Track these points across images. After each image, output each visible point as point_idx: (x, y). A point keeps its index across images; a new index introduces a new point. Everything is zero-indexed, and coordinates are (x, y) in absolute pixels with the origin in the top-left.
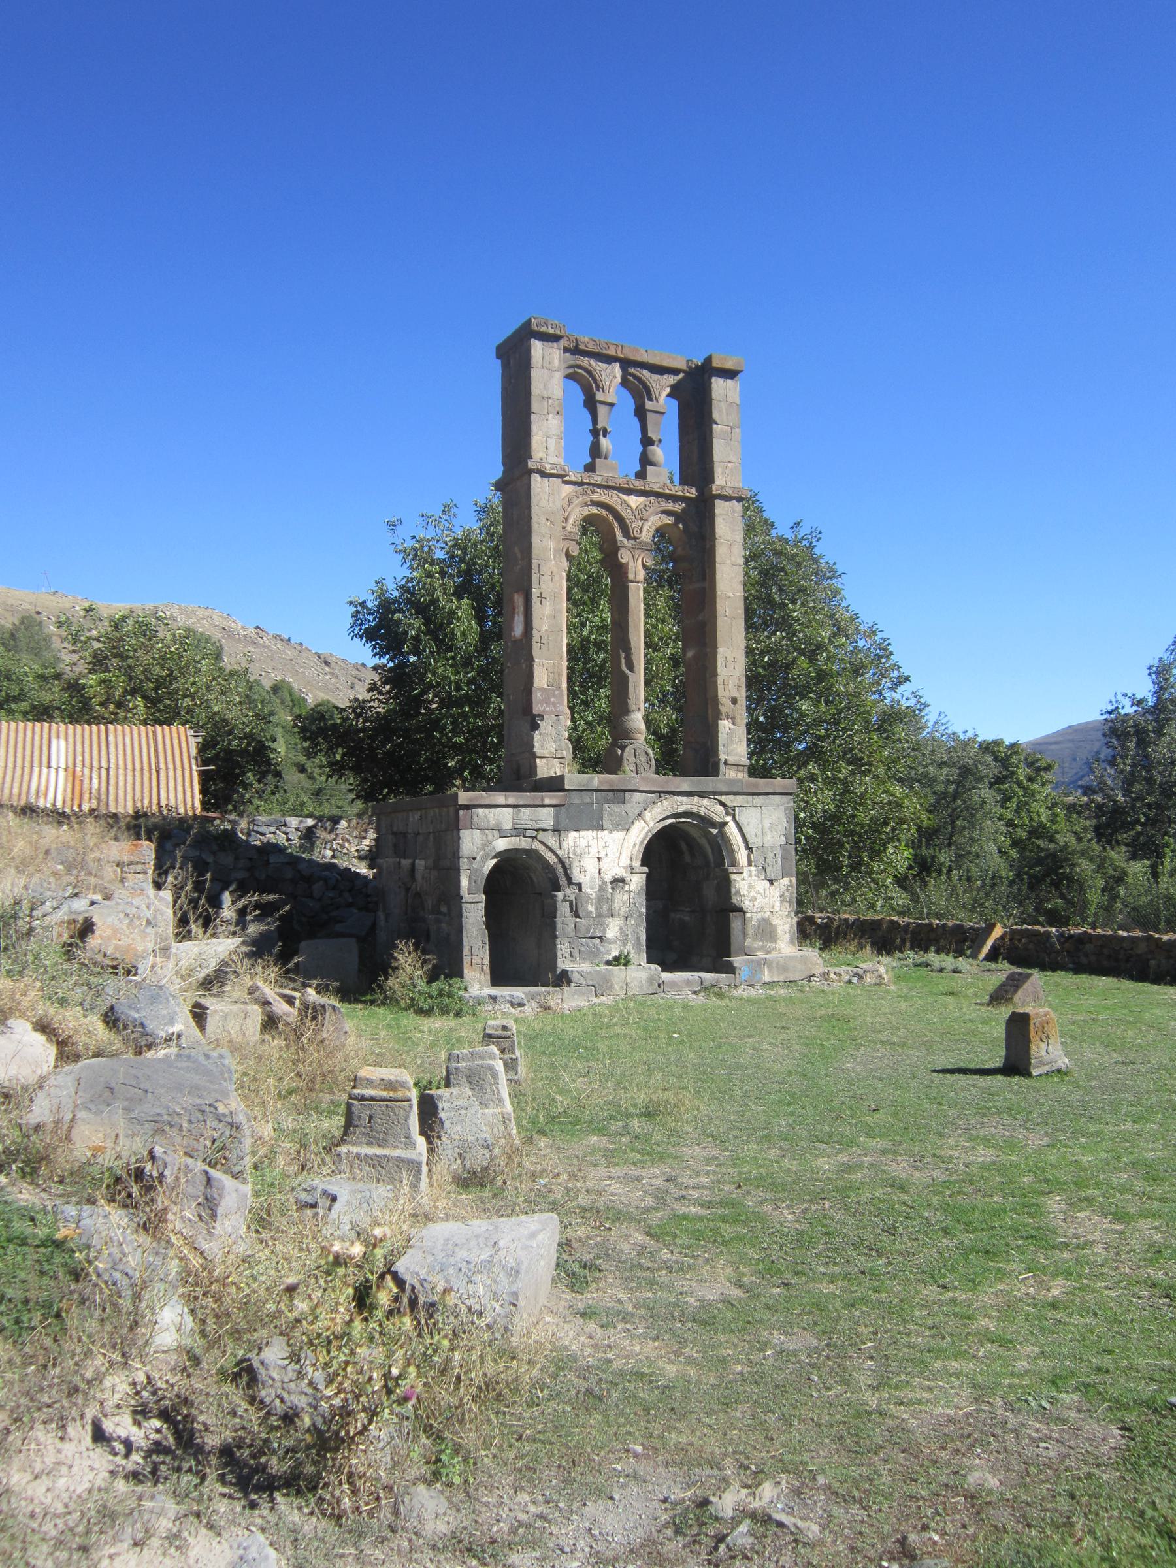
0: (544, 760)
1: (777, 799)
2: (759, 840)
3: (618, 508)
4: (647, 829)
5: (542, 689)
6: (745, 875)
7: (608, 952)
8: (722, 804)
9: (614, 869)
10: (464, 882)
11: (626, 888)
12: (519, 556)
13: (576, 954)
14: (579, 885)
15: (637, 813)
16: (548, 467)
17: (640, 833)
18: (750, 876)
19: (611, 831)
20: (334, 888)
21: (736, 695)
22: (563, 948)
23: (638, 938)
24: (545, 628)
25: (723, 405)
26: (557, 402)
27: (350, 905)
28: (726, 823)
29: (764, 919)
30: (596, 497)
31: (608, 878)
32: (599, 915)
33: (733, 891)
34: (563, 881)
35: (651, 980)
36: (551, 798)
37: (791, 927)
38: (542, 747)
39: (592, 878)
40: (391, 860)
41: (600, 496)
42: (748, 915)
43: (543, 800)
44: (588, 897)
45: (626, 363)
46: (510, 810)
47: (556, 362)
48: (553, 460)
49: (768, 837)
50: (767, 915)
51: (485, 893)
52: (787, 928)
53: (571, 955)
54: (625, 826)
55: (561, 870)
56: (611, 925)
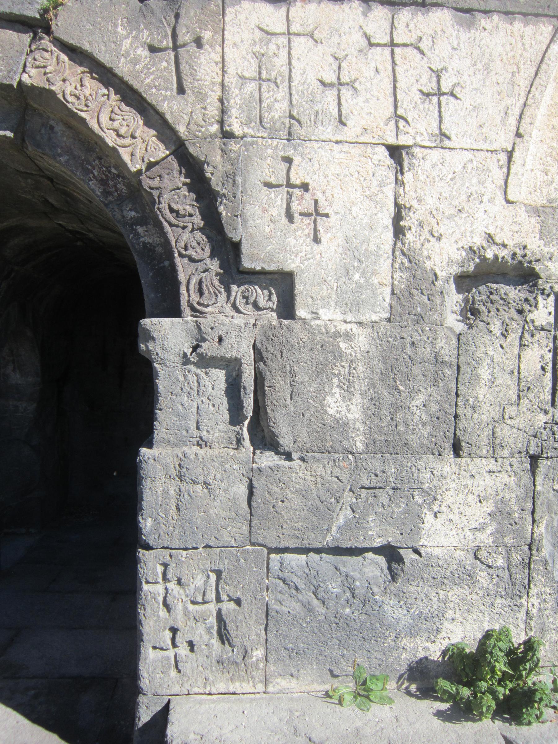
7: (428, 623)
13: (248, 629)
14: (283, 285)
32: (388, 443)
34: (195, 265)
39: (356, 255)
55: (186, 202)
56: (450, 497)
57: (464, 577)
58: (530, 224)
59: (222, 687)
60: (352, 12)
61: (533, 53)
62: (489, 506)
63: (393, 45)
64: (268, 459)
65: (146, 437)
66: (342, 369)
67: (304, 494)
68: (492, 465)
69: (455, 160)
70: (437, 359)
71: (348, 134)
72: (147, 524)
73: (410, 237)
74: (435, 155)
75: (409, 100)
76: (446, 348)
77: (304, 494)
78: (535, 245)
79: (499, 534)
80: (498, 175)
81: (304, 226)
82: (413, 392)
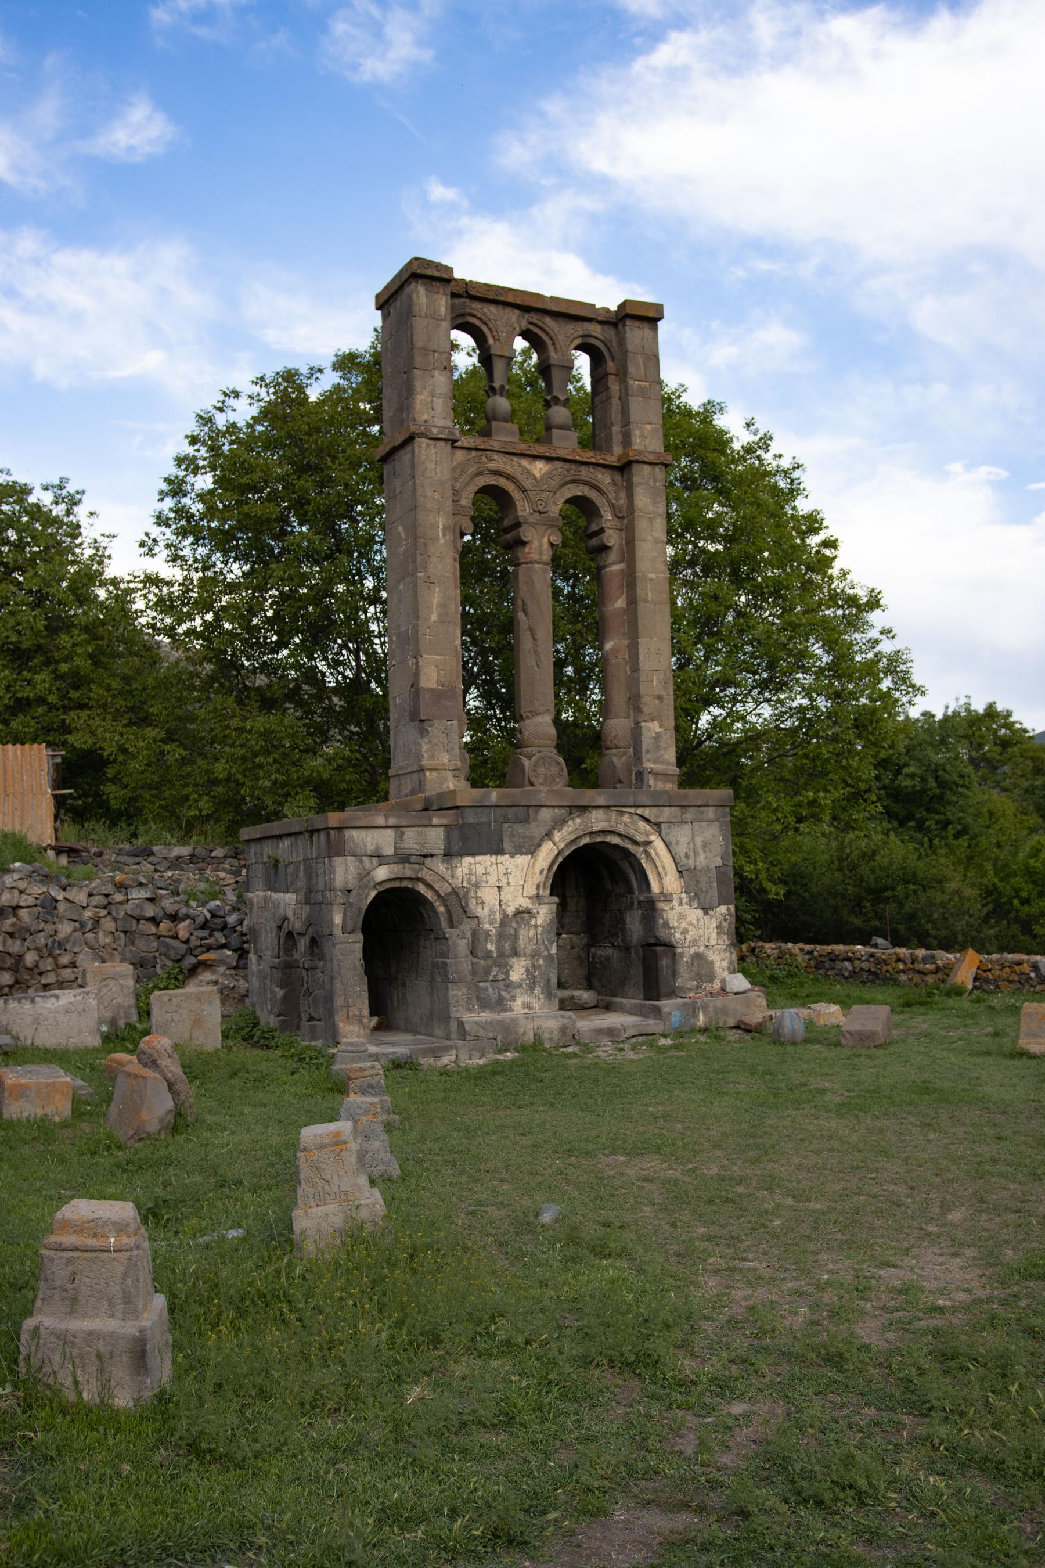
0: (435, 774)
1: (711, 813)
2: (691, 862)
3: (520, 477)
4: (556, 852)
6: (675, 903)
8: (647, 820)
9: (517, 899)
10: (338, 919)
11: (533, 922)
12: (403, 536)
16: (435, 431)
17: (547, 854)
18: (681, 904)
19: (512, 856)
20: (203, 927)
21: (663, 693)
22: (457, 993)
23: (549, 980)
24: (434, 617)
27: (223, 946)
28: (649, 843)
29: (698, 956)
30: (492, 465)
31: (510, 910)
32: (501, 954)
35: (563, 1030)
36: (440, 817)
37: (731, 962)
38: (432, 757)
39: (492, 912)
40: (261, 893)
41: (498, 462)
42: (679, 950)
43: (430, 820)
44: (487, 933)
45: (526, 309)
46: (390, 832)
47: (443, 310)
48: (441, 423)
49: (702, 858)
50: (702, 949)
51: (364, 930)
52: (725, 964)
56: (515, 967)
57: (520, 986)
58: (529, 901)
60: (488, 857)
64: (475, 960)
76: (512, 931)
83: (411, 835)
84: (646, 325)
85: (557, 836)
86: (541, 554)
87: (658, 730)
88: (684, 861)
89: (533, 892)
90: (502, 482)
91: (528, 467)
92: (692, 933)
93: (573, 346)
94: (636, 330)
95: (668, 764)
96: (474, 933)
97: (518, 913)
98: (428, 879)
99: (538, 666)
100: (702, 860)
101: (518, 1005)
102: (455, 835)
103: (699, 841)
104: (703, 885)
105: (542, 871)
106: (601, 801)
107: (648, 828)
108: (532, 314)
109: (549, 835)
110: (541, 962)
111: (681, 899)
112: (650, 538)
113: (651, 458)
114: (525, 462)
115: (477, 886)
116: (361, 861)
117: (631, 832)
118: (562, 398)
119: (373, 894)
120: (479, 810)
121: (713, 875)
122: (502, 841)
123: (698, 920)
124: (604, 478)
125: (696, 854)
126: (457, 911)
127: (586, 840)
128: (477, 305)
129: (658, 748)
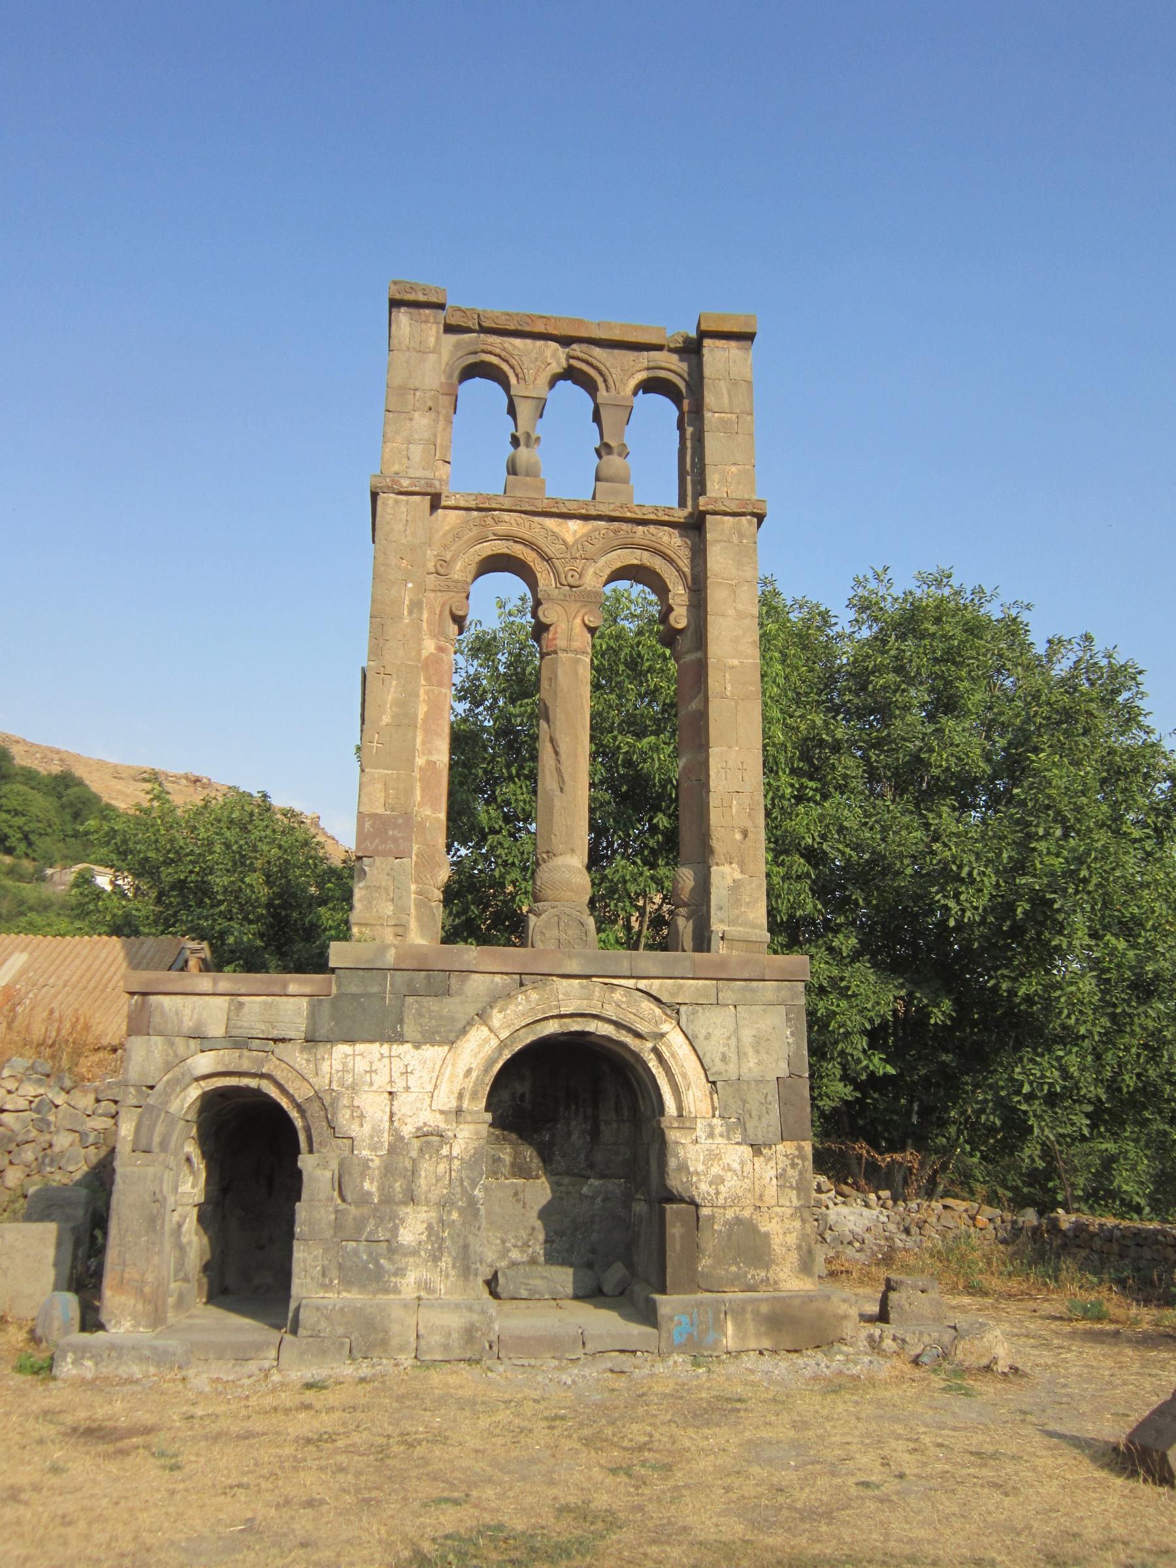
1: (769, 989)
2: (732, 1071)
3: (541, 542)
4: (494, 1043)
5: (374, 816)
8: (657, 1000)
9: (418, 1113)
11: (445, 1151)
15: (472, 1010)
16: (405, 483)
18: (711, 1135)
19: (417, 1046)
21: (748, 824)
23: (466, 1247)
24: (386, 719)
25: (723, 385)
26: (428, 395)
29: (738, 1221)
30: (502, 529)
31: (407, 1131)
32: (387, 1199)
33: (672, 1163)
35: (470, 1334)
36: (300, 982)
38: (368, 907)
39: (376, 1131)
41: (512, 523)
42: (705, 1212)
43: (285, 986)
44: (365, 1163)
46: (223, 1002)
47: (432, 341)
49: (752, 1062)
50: (746, 1213)
52: (792, 1239)
53: (324, 1275)
54: (449, 1035)
57: (415, 1253)
59: (321, 1295)
60: (377, 1045)
61: (442, 1056)
62: (425, 1225)
63: (390, 1057)
64: (343, 1206)
65: (299, 1199)
66: (369, 1172)
67: (355, 1219)
68: (425, 1208)
69: (412, 1097)
70: (406, 1169)
71: (374, 1088)
72: (297, 1230)
73: (395, 1124)
74: (404, 1095)
75: (396, 1075)
76: (408, 1164)
77: (355, 1219)
78: (442, 1125)
79: (429, 1236)
80: (428, 1101)
81: (357, 1121)
82: (396, 1181)
83: (253, 1004)
84: (733, 344)
85: (497, 1018)
86: (570, 639)
87: (738, 875)
88: (718, 1066)
89: (454, 1104)
90: (518, 550)
91: (556, 530)
92: (731, 1184)
93: (633, 383)
94: (719, 354)
95: (754, 926)
96: (341, 1165)
97: (421, 1134)
98: (279, 1076)
99: (562, 790)
100: (751, 1065)
101: (409, 1284)
102: (326, 1010)
103: (747, 1035)
104: (753, 1106)
105: (468, 1072)
106: (573, 967)
107: (658, 1011)
108: (574, 346)
109: (483, 1016)
110: (455, 1215)
111: (711, 1127)
112: (731, 612)
113: (733, 507)
114: (550, 523)
115: (354, 1088)
116: (172, 1044)
117: (629, 1019)
118: (613, 443)
119: (194, 1093)
120: (368, 974)
121: (772, 1089)
122: (401, 1021)
123: (742, 1163)
124: (673, 541)
125: (741, 1054)
126: (319, 1129)
127: (552, 1027)
128: (495, 340)
129: (738, 902)
